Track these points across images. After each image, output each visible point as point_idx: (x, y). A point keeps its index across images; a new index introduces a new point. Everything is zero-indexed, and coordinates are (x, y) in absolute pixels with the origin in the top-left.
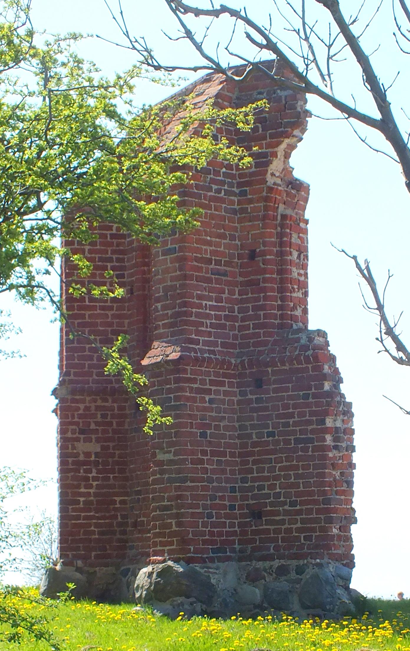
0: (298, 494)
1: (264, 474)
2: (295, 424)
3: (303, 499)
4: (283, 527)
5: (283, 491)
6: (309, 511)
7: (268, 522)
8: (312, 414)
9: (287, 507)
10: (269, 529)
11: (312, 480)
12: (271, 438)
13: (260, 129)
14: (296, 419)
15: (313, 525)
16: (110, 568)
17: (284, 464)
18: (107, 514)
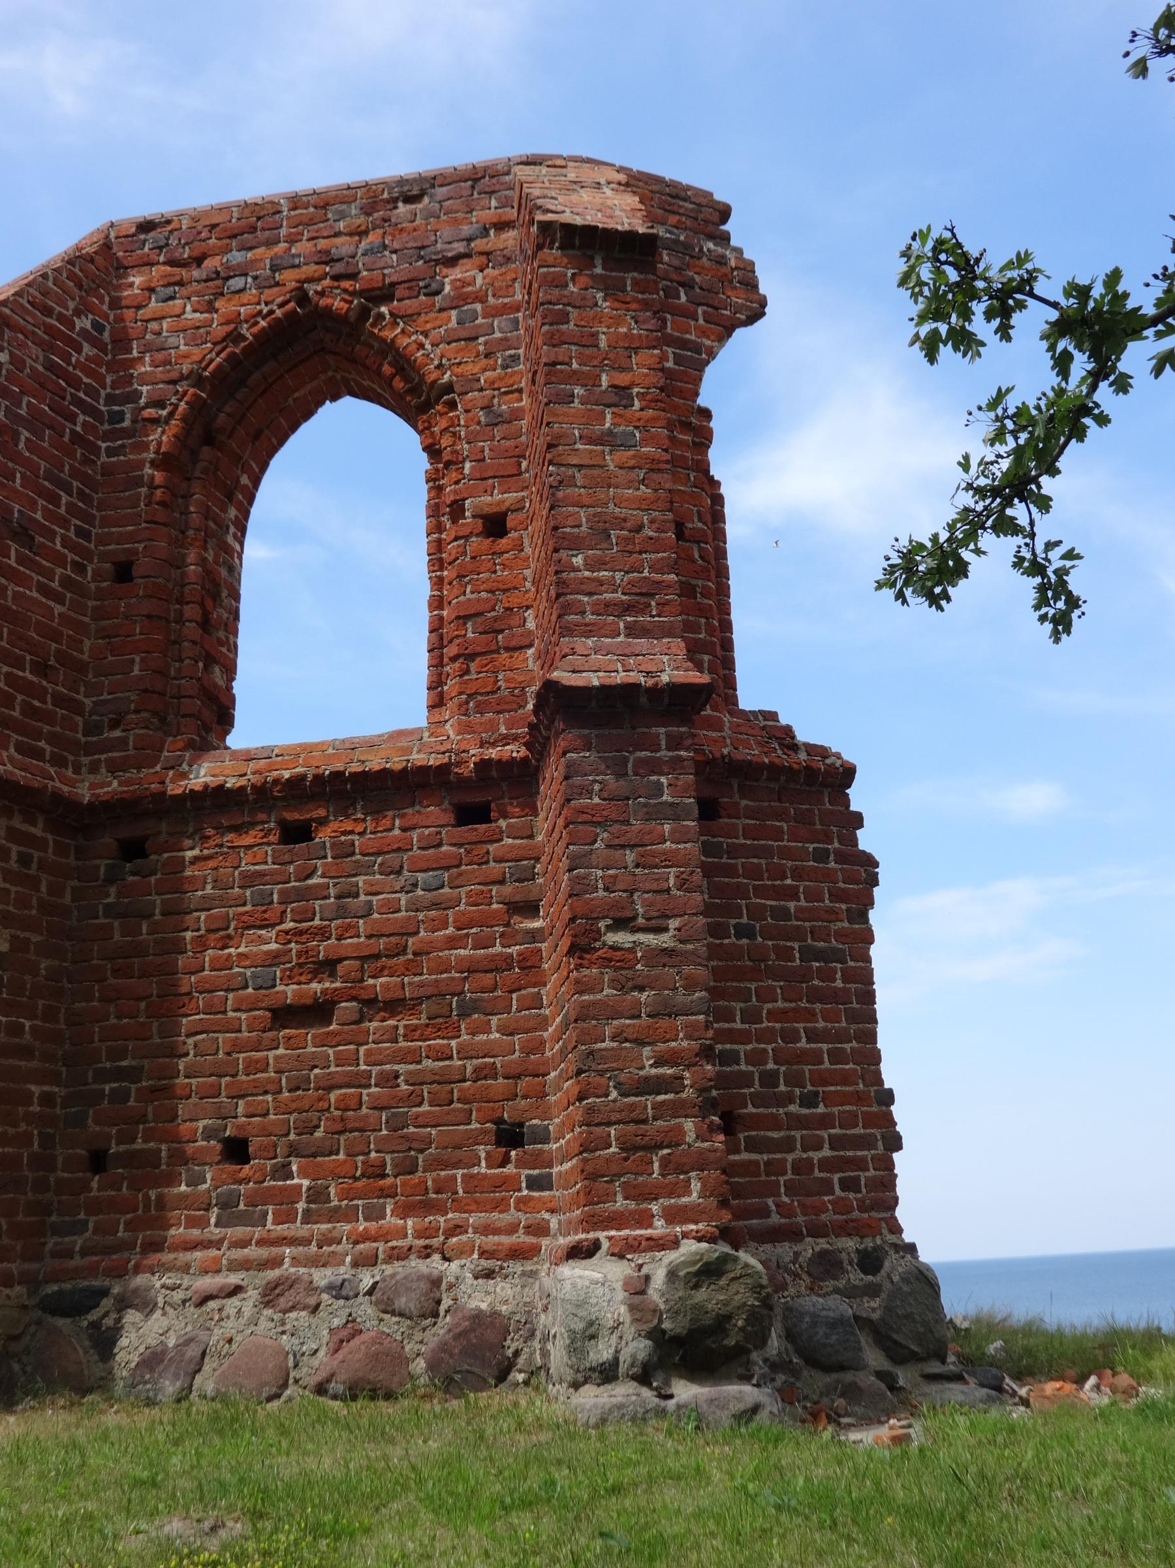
0: (822, 1079)
1: (733, 1025)
2: (801, 914)
3: (832, 1088)
4: (790, 1157)
5: (783, 1068)
6: (849, 1121)
7: (752, 1145)
8: (836, 896)
9: (793, 1108)
10: (757, 1163)
11: (847, 1046)
12: (745, 941)
13: (683, 298)
14: (803, 903)
15: (859, 1153)
16: (18, 1289)
17: (780, 1004)
18: (11, 1131)
